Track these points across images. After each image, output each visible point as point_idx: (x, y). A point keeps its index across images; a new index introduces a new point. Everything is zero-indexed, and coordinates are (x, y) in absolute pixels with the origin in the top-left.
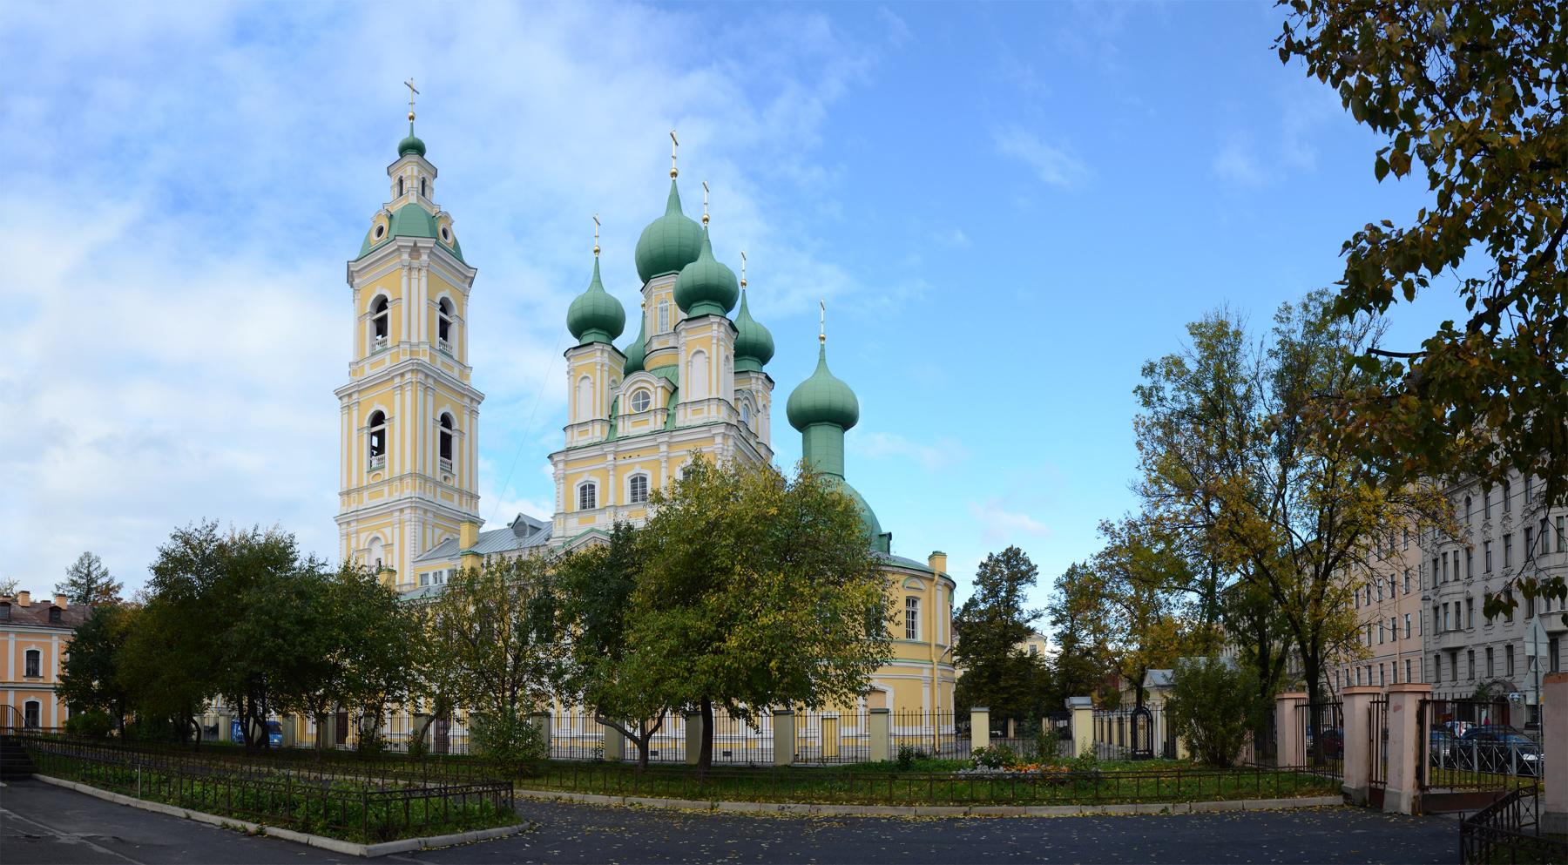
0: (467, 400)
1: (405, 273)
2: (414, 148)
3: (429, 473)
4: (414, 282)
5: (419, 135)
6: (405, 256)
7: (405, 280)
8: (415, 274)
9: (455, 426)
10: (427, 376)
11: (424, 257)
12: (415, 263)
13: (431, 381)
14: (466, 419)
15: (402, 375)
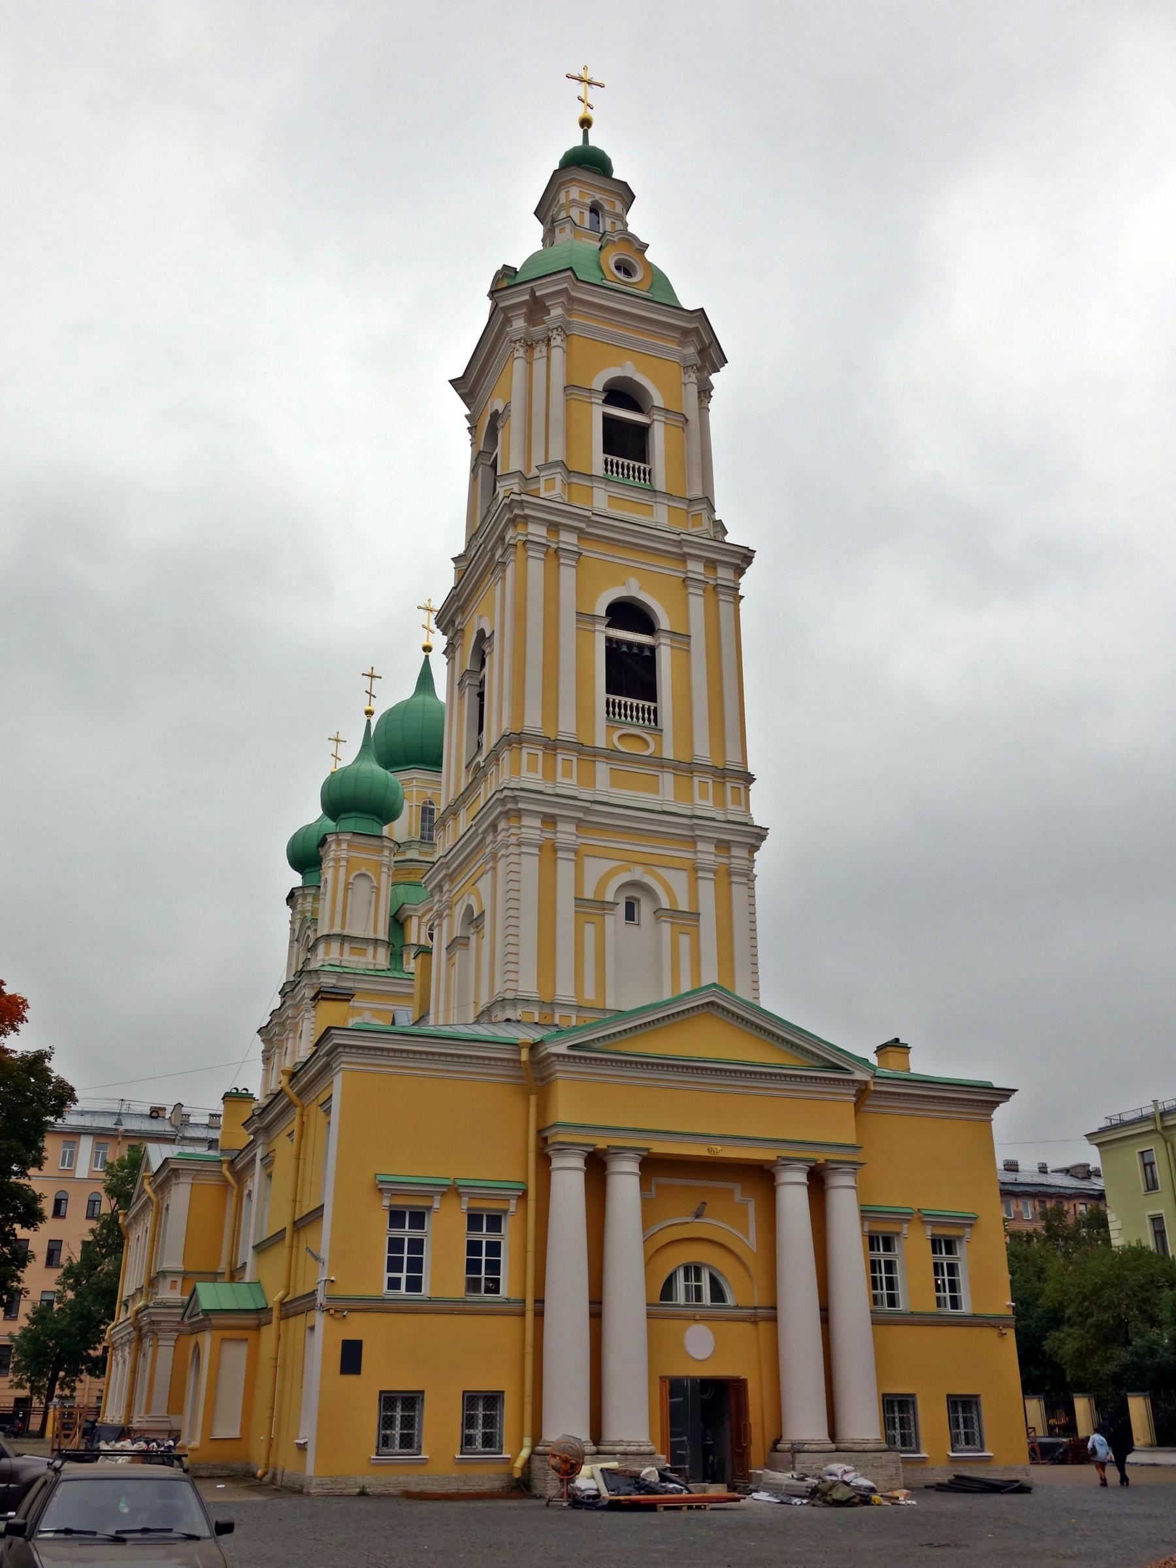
0: (696, 568)
1: (520, 353)
2: (586, 163)
3: (567, 726)
4: (539, 366)
5: (597, 140)
6: (519, 324)
7: (519, 366)
8: (540, 351)
9: (664, 622)
10: (554, 528)
11: (556, 312)
12: (538, 330)
13: (568, 539)
14: (697, 604)
15: (502, 538)
